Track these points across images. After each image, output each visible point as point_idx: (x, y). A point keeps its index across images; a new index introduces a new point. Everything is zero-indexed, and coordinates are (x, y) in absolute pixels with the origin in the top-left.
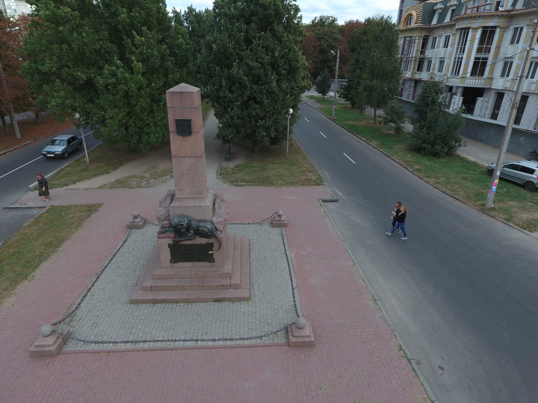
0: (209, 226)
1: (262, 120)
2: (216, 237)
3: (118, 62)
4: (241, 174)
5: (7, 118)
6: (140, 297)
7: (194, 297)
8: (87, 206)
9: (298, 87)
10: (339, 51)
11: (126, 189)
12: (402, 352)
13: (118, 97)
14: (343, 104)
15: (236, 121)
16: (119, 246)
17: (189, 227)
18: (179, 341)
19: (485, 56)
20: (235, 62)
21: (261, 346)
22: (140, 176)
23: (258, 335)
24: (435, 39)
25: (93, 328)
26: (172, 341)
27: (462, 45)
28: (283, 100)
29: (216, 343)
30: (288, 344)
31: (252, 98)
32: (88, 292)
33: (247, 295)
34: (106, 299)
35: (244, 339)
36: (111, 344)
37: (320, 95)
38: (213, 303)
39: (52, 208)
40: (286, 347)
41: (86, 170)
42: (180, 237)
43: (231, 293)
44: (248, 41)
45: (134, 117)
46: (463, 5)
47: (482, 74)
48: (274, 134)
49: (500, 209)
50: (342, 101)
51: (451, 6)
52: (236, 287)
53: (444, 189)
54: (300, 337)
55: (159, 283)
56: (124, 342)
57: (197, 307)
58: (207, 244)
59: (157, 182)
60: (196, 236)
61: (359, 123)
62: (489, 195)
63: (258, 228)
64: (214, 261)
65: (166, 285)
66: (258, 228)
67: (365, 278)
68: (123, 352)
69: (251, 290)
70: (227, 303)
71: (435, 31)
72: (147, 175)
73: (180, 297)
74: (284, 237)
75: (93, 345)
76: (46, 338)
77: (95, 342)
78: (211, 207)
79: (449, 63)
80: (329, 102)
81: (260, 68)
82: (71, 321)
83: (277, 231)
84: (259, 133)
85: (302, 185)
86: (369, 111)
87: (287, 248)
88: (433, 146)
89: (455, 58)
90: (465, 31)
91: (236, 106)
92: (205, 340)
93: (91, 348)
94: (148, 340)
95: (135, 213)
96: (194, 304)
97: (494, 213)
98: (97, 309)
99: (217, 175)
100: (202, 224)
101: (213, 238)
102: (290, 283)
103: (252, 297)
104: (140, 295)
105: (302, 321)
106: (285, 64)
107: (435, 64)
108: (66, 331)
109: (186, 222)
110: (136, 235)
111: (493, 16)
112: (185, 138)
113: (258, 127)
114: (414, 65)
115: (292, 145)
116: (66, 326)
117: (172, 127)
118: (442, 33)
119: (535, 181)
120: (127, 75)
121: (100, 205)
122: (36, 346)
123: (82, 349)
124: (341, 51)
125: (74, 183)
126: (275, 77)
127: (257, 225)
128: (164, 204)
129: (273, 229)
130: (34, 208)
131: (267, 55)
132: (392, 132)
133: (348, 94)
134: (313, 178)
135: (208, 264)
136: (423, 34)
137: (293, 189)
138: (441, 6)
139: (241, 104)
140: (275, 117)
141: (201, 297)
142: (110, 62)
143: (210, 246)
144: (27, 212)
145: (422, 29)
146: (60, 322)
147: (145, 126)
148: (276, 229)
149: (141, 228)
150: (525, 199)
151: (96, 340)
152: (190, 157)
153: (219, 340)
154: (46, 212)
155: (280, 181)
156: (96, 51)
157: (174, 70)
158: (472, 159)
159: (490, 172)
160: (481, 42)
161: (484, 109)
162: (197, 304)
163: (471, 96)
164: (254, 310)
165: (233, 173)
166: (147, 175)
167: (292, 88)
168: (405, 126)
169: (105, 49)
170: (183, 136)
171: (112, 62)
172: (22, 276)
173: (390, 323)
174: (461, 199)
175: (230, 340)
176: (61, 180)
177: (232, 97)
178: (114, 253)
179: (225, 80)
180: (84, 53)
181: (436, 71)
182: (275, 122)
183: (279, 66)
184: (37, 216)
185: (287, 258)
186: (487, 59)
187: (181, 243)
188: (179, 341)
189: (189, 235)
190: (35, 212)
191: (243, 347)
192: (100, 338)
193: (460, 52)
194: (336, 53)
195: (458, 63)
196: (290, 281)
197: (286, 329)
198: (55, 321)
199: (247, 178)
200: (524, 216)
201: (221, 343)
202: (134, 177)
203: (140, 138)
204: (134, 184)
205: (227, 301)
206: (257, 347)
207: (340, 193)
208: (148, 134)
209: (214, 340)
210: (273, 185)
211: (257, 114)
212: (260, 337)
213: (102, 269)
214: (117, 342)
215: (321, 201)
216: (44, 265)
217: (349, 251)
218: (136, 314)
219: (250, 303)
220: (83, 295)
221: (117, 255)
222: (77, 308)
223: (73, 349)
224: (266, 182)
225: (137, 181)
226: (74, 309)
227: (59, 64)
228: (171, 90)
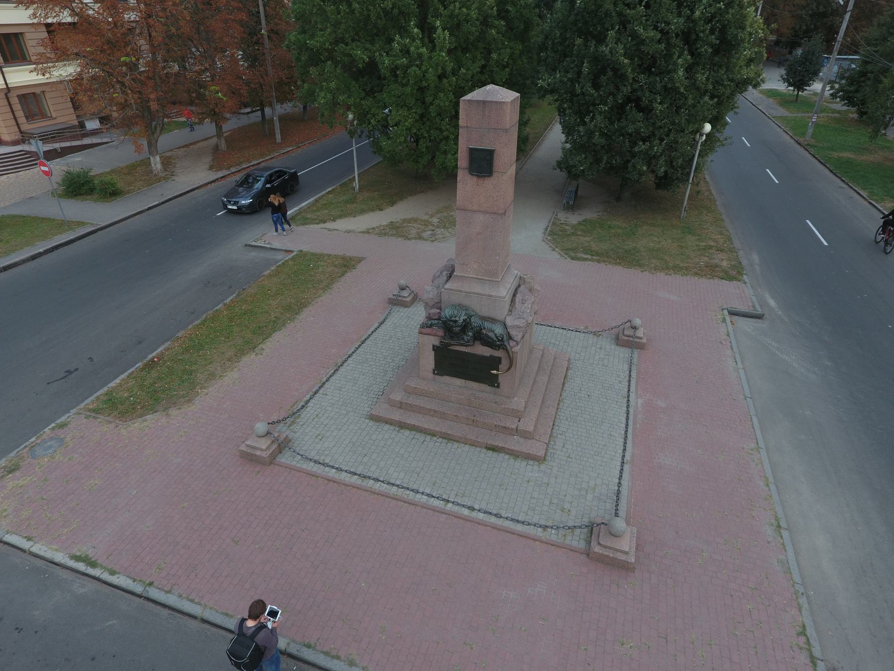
0: (499, 330)
1: (644, 140)
2: (507, 350)
3: (416, 30)
4: (588, 239)
5: (268, 110)
7: (458, 434)
8: (344, 258)
9: (732, 80)
11: (400, 239)
12: (802, 639)
13: (408, 90)
14: (839, 112)
15: (597, 139)
16: (373, 329)
17: (466, 326)
18: (423, 493)
20: (613, 29)
21: (542, 542)
22: (425, 221)
23: (542, 522)
25: (317, 440)
26: (412, 490)
28: (694, 106)
29: (474, 514)
30: (588, 553)
31: (634, 100)
32: (320, 388)
33: (541, 453)
34: (340, 403)
35: (518, 521)
36: (334, 471)
37: (792, 88)
38: (484, 450)
39: (302, 254)
41: (352, 201)
42: (452, 338)
43: (515, 443)
45: (428, 123)
48: (663, 169)
50: (839, 106)
52: (526, 435)
54: (610, 548)
55: (412, 400)
56: (351, 473)
57: (459, 450)
58: (492, 357)
59: (447, 234)
60: (477, 342)
61: (864, 157)
63: (590, 342)
64: (498, 387)
65: (422, 405)
66: (590, 342)
67: (771, 480)
68: (346, 485)
69: (551, 446)
70: (507, 457)
72: (435, 220)
73: (438, 429)
74: (634, 368)
75: (312, 464)
76: (259, 439)
77: (315, 462)
78: (508, 299)
80: (807, 105)
81: (659, 42)
82: (293, 422)
84: (634, 166)
85: (696, 274)
87: (633, 389)
91: (600, 113)
92: (458, 504)
93: (309, 468)
94: (381, 479)
95: (403, 282)
96: (456, 445)
98: (326, 415)
99: (544, 233)
100: (487, 325)
101: (501, 350)
102: (620, 451)
103: (548, 458)
104: (383, 410)
105: (619, 524)
106: (712, 32)
108: (284, 436)
109: (462, 318)
110: (399, 315)
112: (481, 181)
113: (634, 155)
115: (698, 192)
116: (285, 428)
117: (463, 160)
121: (360, 260)
122: (247, 446)
123: (299, 465)
125: (334, 220)
126: (685, 60)
127: (591, 336)
128: (437, 282)
129: (618, 348)
130: (279, 250)
131: (679, 15)
133: (857, 91)
134: (725, 264)
137: (677, 279)
139: (611, 109)
141: (469, 437)
142: (403, 31)
143: (495, 362)
146: (279, 422)
147: (441, 140)
148: (622, 349)
151: (316, 458)
152: (485, 212)
153: (479, 511)
154: (292, 259)
155: (654, 261)
157: (503, 44)
162: (461, 445)
164: (546, 481)
165: (573, 234)
166: (435, 220)
167: (717, 83)
169: (399, 9)
170: (478, 176)
171: (406, 31)
172: (249, 346)
173: (797, 578)
175: (495, 515)
176: (318, 213)
177: (596, 95)
178: (363, 339)
179: (588, 62)
180: (369, 16)
182: (671, 147)
183: (697, 35)
185: (628, 407)
187: (451, 348)
188: (423, 493)
189: (465, 337)
190: (279, 256)
191: (514, 534)
192: (323, 457)
196: (622, 448)
197: (592, 529)
199: (594, 247)
201: (481, 516)
202: (415, 220)
203: (433, 158)
204: (413, 232)
205: (507, 453)
206: (535, 540)
207: (772, 303)
210: (640, 266)
211: (637, 132)
212: (545, 527)
214: (341, 470)
215: (726, 312)
216: (278, 336)
217: (755, 420)
218: (374, 437)
219: (543, 467)
220: (314, 390)
221: (368, 342)
222: (303, 406)
223: (288, 462)
224: (627, 258)
225: (418, 228)
226: (299, 407)
227: (334, 35)
228: (469, 97)
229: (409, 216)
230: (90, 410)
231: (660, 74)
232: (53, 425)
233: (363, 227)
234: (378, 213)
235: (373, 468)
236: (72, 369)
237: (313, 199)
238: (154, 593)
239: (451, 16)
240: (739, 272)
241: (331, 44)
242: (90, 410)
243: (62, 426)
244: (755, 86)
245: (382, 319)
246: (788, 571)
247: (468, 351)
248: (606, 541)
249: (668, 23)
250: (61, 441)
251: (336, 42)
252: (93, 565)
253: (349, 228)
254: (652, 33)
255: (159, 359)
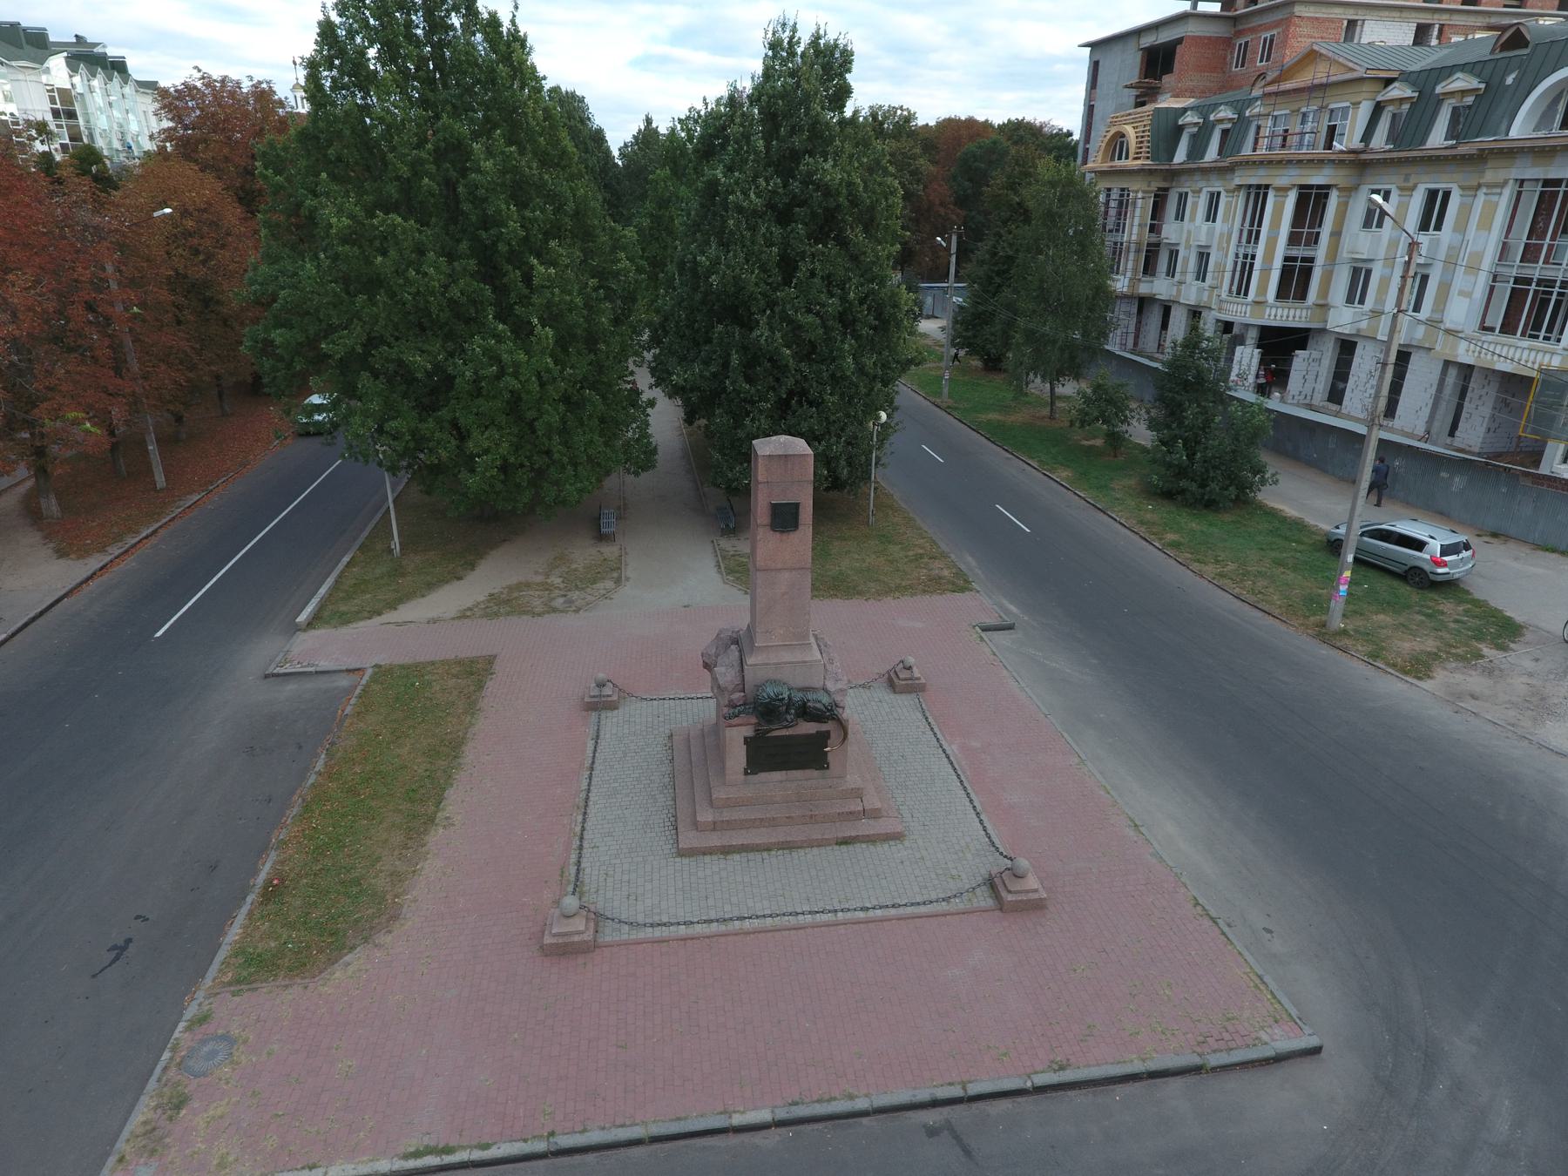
0: (826, 700)
6: (696, 844)
8: (459, 662)
10: (954, 238)
19: (1308, 253)
22: (542, 584)
24: (1183, 198)
27: (1252, 224)
28: (868, 395)
29: (871, 914)
33: (899, 829)
40: (997, 913)
42: (769, 722)
43: (866, 827)
44: (788, 265)
46: (1250, 122)
47: (1302, 295)
49: (1356, 631)
51: (1221, 121)
52: (875, 814)
53: (1237, 590)
55: (727, 815)
59: (589, 598)
62: (1333, 603)
71: (1183, 178)
77: (652, 925)
79: (1224, 260)
83: (905, 701)
86: (1038, 386)
88: (1203, 485)
89: (1237, 256)
90: (1258, 194)
95: (601, 676)
96: (801, 852)
97: (1346, 642)
104: (689, 839)
105: (1023, 863)
106: (869, 309)
107: (1186, 260)
110: (610, 721)
111: (1321, 161)
112: (785, 536)
114: (1136, 261)
118: (1201, 184)
119: (1427, 567)
120: (522, 357)
121: (491, 660)
124: (959, 237)
125: (392, 606)
131: (832, 296)
132: (1099, 442)
134: (946, 573)
135: (816, 773)
136: (1156, 184)
138: (1196, 120)
140: (850, 430)
143: (824, 737)
144: (322, 683)
145: (1151, 172)
148: (903, 697)
149: (616, 708)
150: (1409, 607)
151: (649, 920)
152: (792, 569)
154: (374, 679)
156: (452, 303)
158: (1290, 511)
159: (1334, 546)
160: (1298, 220)
161: (1311, 377)
163: (1279, 345)
168: (1130, 429)
174: (1276, 612)
177: (753, 391)
178: (587, 763)
181: (1190, 277)
184: (358, 691)
186: (1312, 260)
193: (1249, 242)
194: (949, 244)
195: (1245, 269)
197: (991, 884)
198: (570, 888)
200: (1407, 645)
201: (879, 912)
202: (528, 585)
206: (944, 915)
208: (556, 483)
209: (868, 909)
210: (860, 593)
213: (583, 795)
216: (451, 794)
219: (907, 843)
229: (514, 580)
230: (230, 984)
231: (822, 361)
232: (182, 1025)
233: (452, 611)
234: (456, 583)
235: (727, 908)
236: (121, 942)
237: (330, 581)
238: (565, 1141)
239: (549, 305)
240: (966, 581)
241: (364, 345)
242: (230, 984)
243: (202, 1020)
244: (917, 365)
245: (592, 732)
246: (1161, 860)
247: (788, 734)
248: (1015, 885)
249: (823, 305)
250: (227, 1038)
251: (372, 342)
252: (448, 1150)
253: (430, 615)
254: (810, 318)
255: (282, 881)
